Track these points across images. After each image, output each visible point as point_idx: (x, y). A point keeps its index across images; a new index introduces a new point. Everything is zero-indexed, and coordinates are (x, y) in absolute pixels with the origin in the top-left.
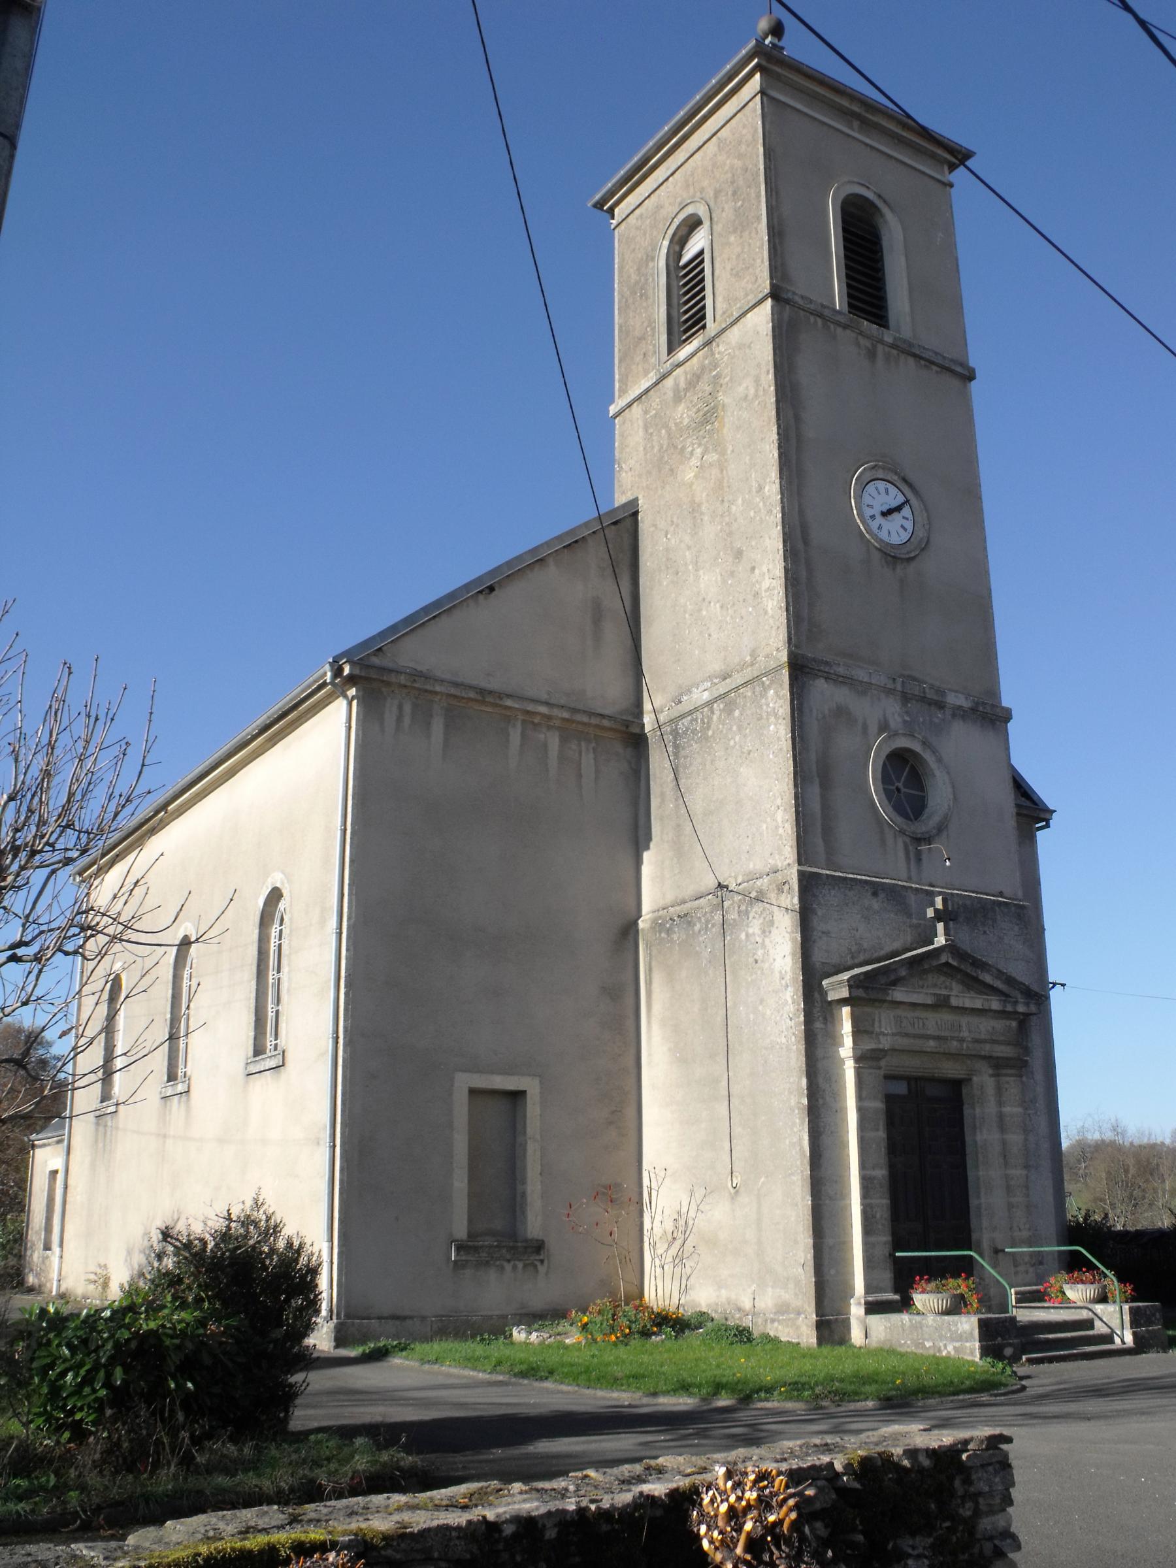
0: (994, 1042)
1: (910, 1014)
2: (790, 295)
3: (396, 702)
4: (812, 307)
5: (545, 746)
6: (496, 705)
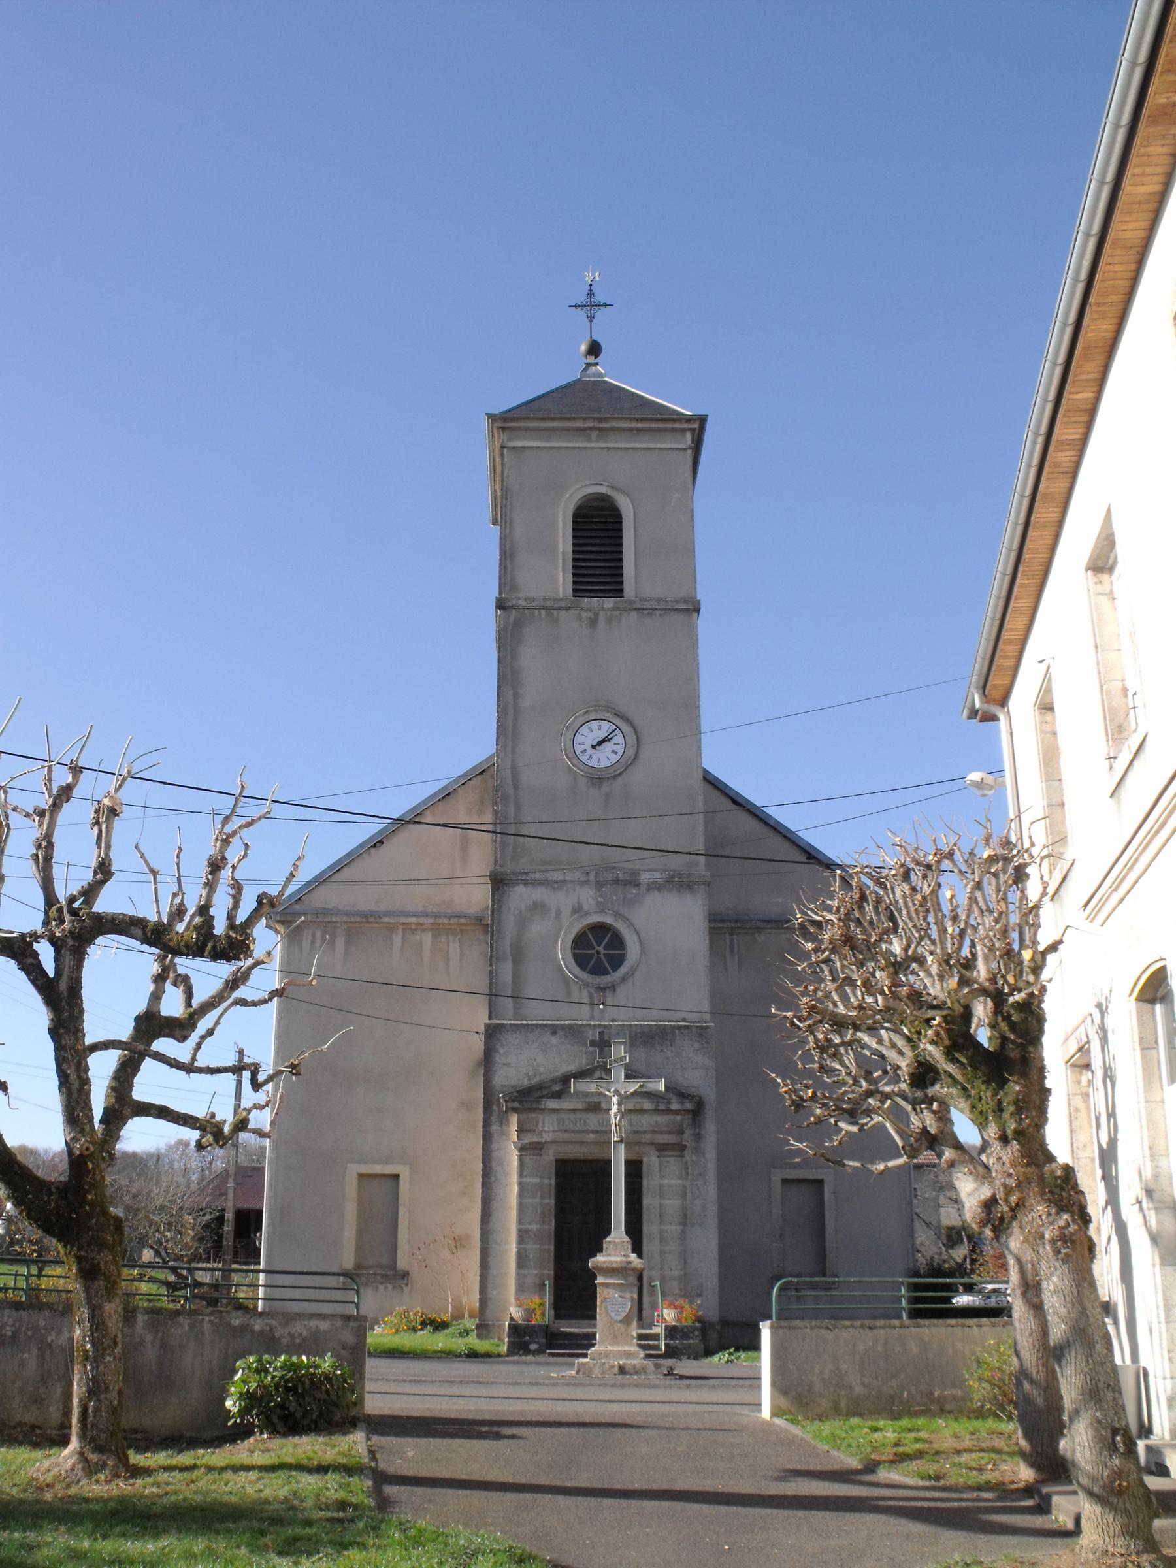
0: (654, 1132)
1: (572, 1116)
2: (514, 602)
3: (311, 932)
4: (534, 604)
5: (421, 944)
6: (379, 923)
